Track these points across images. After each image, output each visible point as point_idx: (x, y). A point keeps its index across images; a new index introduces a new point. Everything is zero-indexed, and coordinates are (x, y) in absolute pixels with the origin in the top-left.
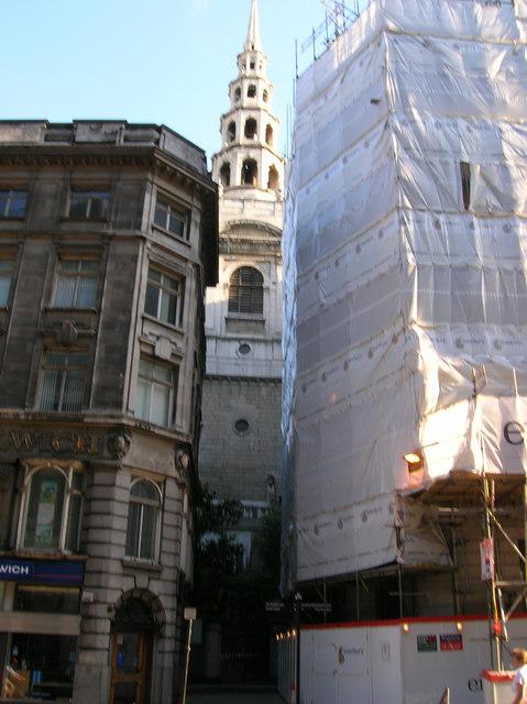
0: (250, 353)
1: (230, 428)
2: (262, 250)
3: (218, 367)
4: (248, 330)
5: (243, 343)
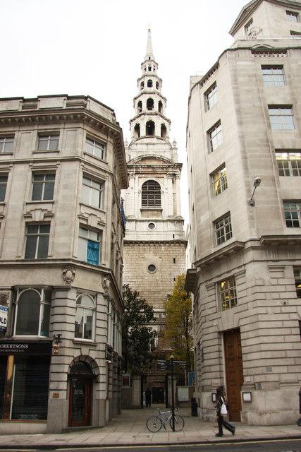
2: (159, 171)
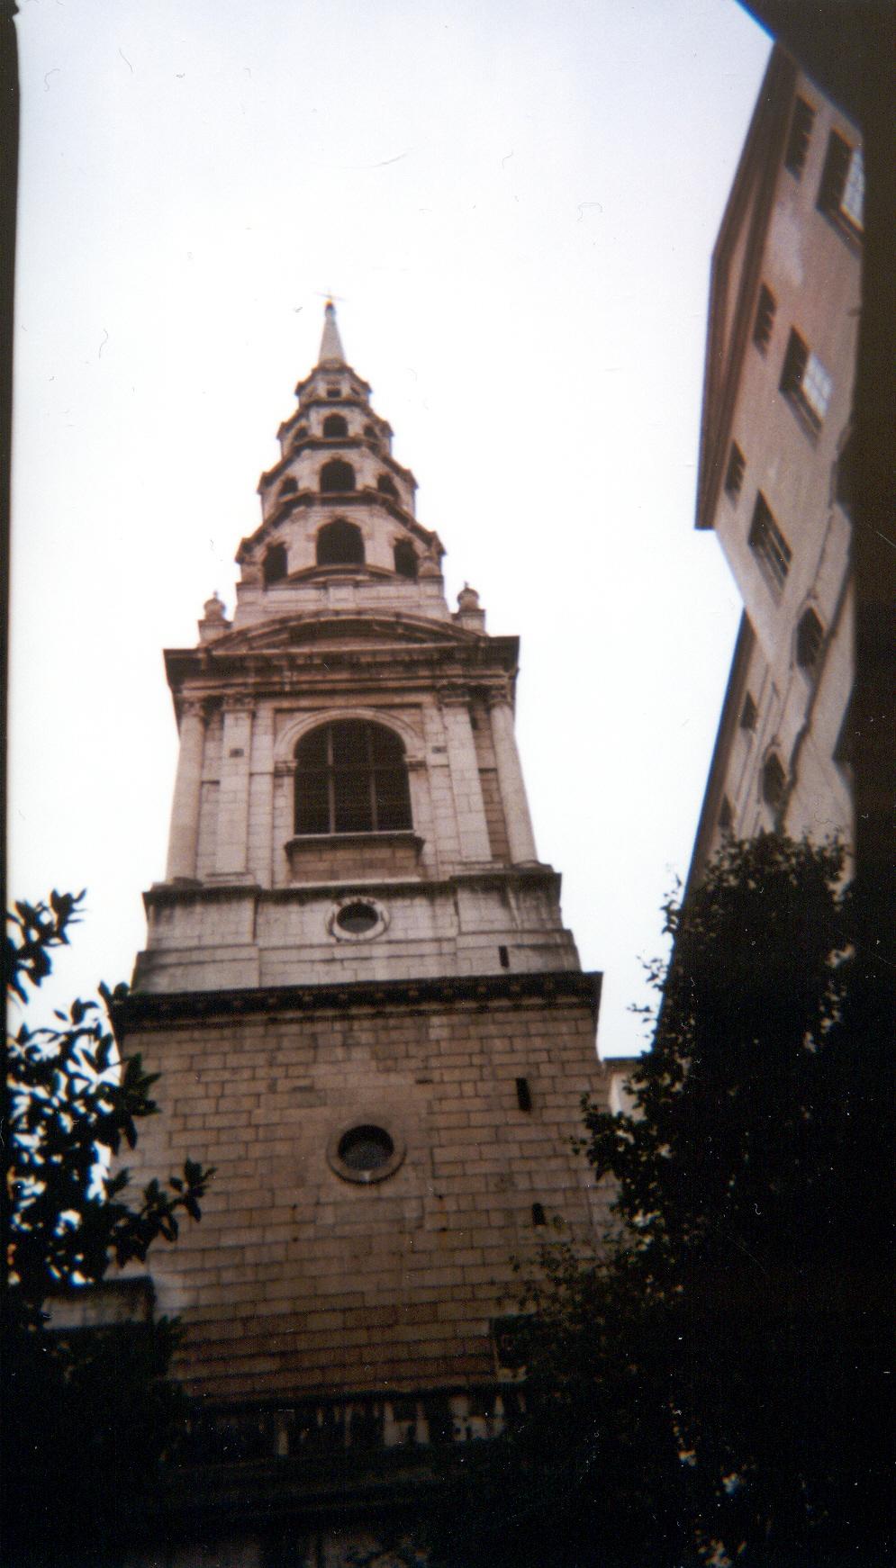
0: (379, 926)
1: (321, 1164)
2: (390, 678)
3: (261, 974)
4: (370, 866)
5: (347, 901)
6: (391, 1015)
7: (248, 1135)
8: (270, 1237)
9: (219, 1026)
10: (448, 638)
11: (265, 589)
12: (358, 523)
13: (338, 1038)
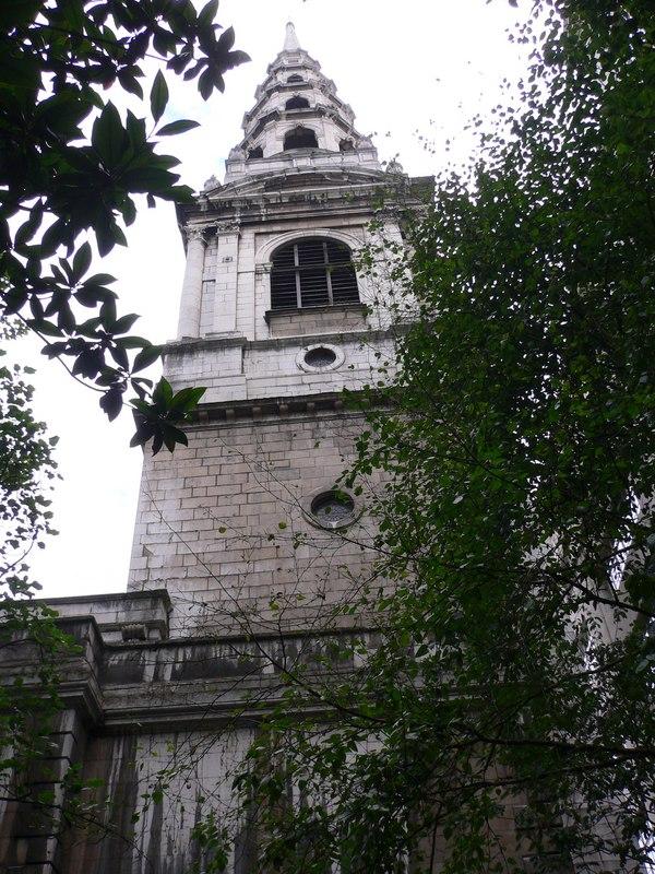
0: (337, 363)
5: (310, 348)
6: (348, 417)
7: (241, 499)
8: (258, 568)
9: (218, 428)
10: (378, 180)
11: (247, 164)
12: (312, 128)
13: (309, 434)
